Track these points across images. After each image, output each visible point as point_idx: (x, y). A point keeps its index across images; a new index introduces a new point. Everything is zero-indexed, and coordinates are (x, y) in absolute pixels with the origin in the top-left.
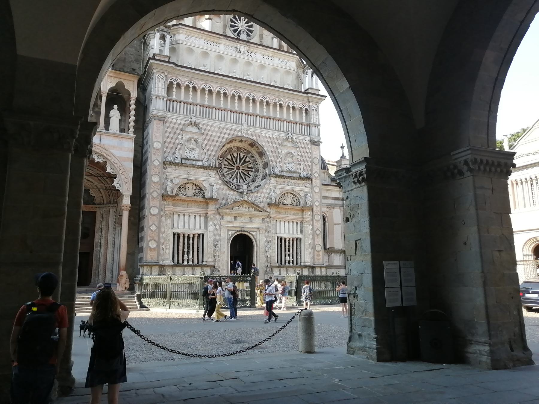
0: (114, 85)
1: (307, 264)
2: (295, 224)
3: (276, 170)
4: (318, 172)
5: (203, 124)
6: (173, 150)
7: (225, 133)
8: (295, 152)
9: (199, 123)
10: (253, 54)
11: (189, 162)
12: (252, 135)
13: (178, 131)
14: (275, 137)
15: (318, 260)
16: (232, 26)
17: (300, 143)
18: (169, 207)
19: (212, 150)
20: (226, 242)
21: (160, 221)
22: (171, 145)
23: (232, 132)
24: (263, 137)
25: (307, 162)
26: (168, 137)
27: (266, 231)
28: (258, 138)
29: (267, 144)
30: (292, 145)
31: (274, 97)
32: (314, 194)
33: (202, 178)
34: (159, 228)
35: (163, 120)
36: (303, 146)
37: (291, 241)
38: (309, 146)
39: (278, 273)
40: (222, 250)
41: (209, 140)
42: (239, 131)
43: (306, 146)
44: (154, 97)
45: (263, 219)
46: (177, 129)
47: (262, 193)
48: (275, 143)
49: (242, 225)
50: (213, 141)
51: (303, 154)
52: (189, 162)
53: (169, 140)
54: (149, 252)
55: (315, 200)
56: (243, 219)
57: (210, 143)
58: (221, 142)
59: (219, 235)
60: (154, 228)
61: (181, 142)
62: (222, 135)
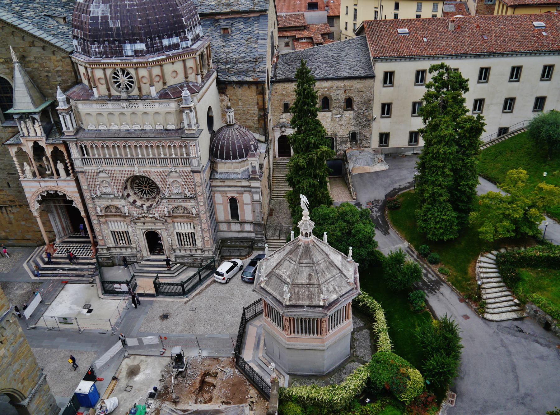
0: (52, 150)
1: (199, 248)
2: (189, 224)
3: (166, 194)
4: (201, 191)
5: (109, 170)
6: (95, 188)
7: (125, 174)
8: (180, 180)
9: (106, 170)
10: (136, 105)
11: (105, 196)
12: (144, 172)
13: (95, 177)
14: (161, 171)
15: (208, 245)
16: (116, 82)
17: (183, 173)
18: (103, 220)
19: (119, 186)
20: (142, 235)
21: (100, 226)
22: (93, 186)
23: (130, 172)
24: (153, 173)
25: (191, 185)
26: (90, 181)
27: (166, 230)
28: (149, 173)
29: (157, 177)
30: (177, 175)
31: (156, 141)
32: (200, 206)
33: (117, 203)
34: (101, 230)
35: (83, 172)
36: (186, 174)
37: (187, 234)
38: (191, 174)
39: (179, 252)
40: (140, 240)
41: (115, 180)
42: (134, 171)
43: (188, 174)
44: (73, 159)
45: (163, 224)
46: (94, 176)
47: (159, 208)
48: (163, 175)
49: (149, 227)
50: (118, 180)
51: (187, 180)
52: (105, 196)
53: (91, 183)
54: (99, 241)
55: (201, 210)
56: (149, 224)
57: (116, 181)
58: (123, 180)
59: (136, 233)
60: (98, 230)
61: (98, 183)
62: (123, 175)
